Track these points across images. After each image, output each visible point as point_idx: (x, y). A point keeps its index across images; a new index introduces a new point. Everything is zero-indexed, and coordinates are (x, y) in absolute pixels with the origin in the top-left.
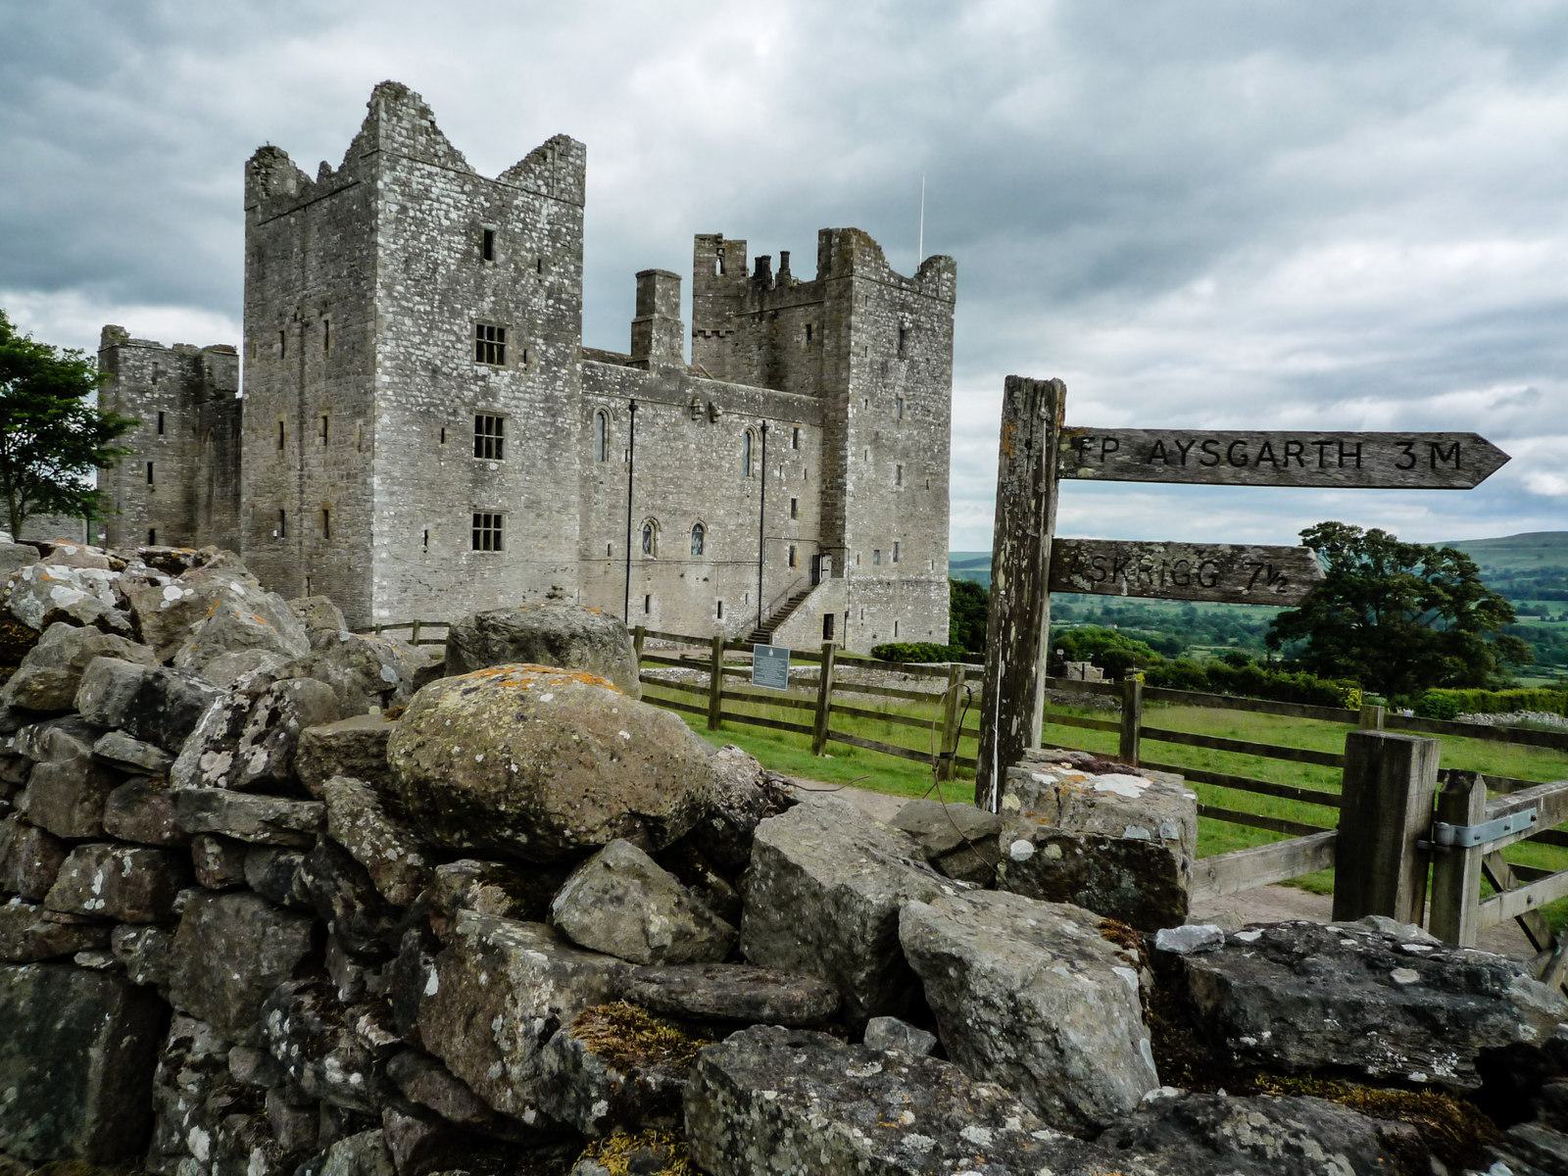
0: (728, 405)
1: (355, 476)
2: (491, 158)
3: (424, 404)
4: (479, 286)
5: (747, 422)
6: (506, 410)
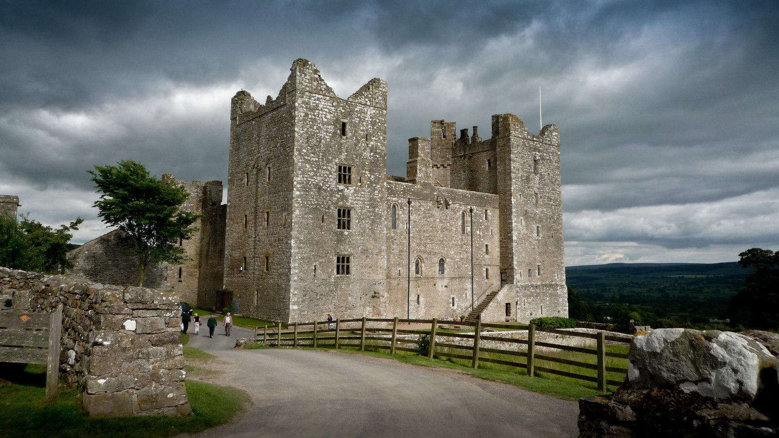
0: (454, 200)
3: (315, 204)
4: (340, 148)
5: (463, 208)
6: (352, 206)
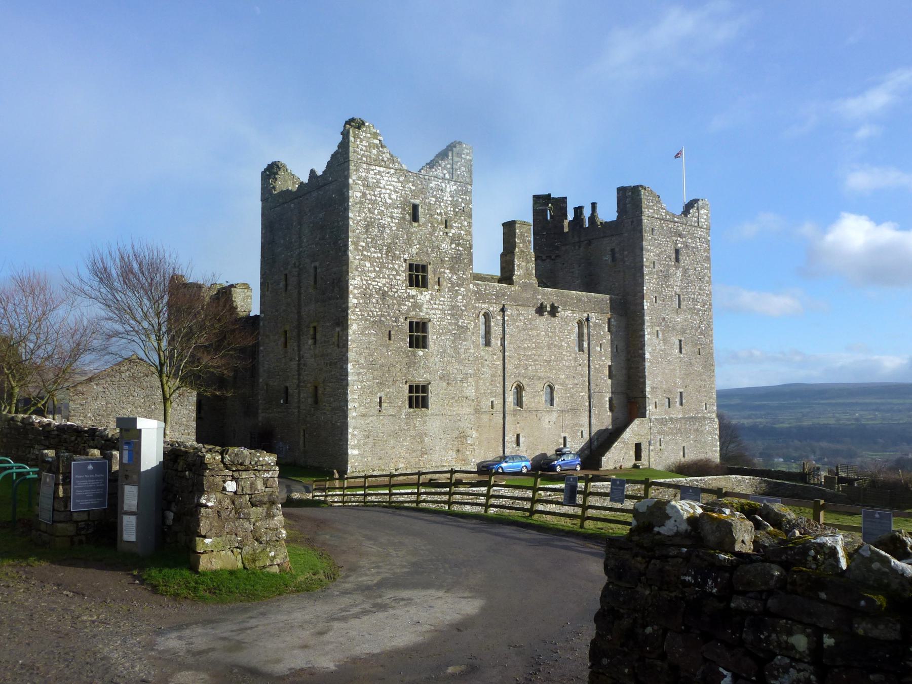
1: (335, 364)
4: (409, 239)
5: (577, 316)
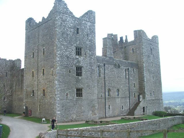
0: (122, 64)
2: (78, 14)
4: (76, 39)
5: (125, 68)
